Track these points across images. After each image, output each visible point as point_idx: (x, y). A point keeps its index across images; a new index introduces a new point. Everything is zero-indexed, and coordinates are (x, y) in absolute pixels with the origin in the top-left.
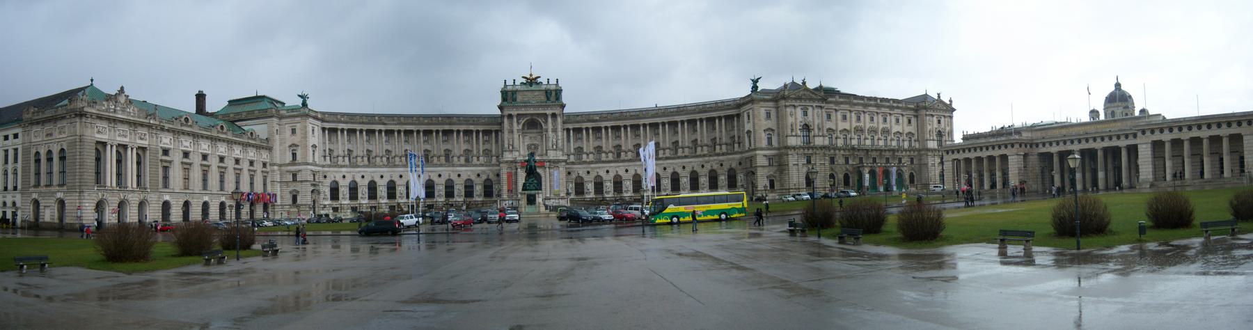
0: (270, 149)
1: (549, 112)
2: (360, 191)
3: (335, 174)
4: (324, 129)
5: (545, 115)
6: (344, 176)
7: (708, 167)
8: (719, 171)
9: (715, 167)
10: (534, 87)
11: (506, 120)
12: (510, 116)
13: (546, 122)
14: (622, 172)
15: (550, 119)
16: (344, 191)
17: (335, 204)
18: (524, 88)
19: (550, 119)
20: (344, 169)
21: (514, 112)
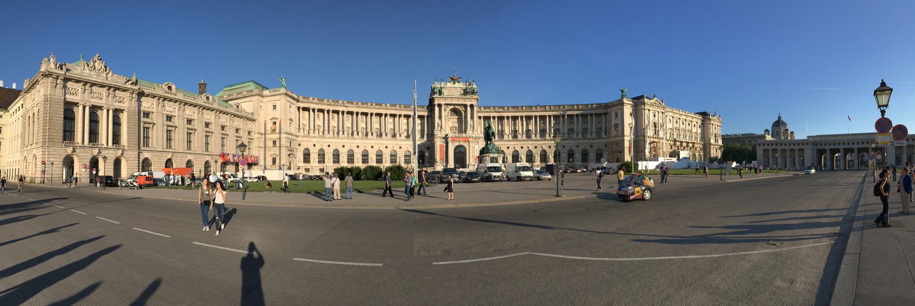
0: (253, 120)
1: (468, 103)
2: (326, 157)
3: (307, 143)
4: (299, 108)
5: (465, 106)
6: (315, 143)
7: (581, 147)
8: (589, 150)
9: (587, 147)
10: (457, 85)
11: (437, 109)
12: (440, 105)
13: (466, 111)
14: (518, 149)
15: (469, 109)
16: (314, 157)
17: (307, 166)
18: (449, 85)
19: (469, 109)
20: (314, 140)
21: (442, 102)
